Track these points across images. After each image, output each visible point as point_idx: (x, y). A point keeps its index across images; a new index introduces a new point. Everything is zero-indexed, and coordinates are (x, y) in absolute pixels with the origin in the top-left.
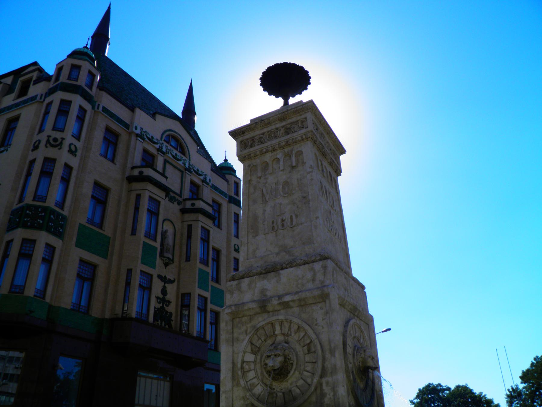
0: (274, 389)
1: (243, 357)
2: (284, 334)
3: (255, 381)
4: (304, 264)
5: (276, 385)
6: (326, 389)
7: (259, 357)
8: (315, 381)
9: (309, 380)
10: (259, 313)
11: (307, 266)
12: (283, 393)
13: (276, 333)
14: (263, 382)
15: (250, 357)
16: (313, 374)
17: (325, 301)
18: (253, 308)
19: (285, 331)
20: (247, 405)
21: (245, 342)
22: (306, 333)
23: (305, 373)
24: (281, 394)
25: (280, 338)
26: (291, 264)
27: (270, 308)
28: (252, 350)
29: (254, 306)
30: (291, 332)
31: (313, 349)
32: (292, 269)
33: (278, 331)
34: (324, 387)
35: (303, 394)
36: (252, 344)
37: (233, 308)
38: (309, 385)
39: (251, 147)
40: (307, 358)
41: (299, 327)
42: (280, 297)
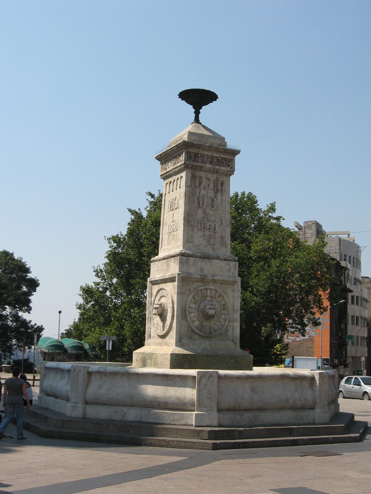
1: (190, 304)
3: (194, 318)
4: (225, 260)
6: (230, 329)
7: (197, 306)
8: (226, 324)
9: (223, 323)
14: (198, 320)
15: (193, 306)
16: (225, 320)
17: (234, 285)
19: (212, 295)
21: (191, 296)
22: (223, 299)
23: (221, 319)
24: (208, 328)
26: (218, 258)
28: (194, 301)
30: (216, 296)
34: (228, 327)
35: (219, 329)
36: (194, 298)
38: (223, 325)
39: (194, 161)
40: (222, 312)
41: (220, 295)
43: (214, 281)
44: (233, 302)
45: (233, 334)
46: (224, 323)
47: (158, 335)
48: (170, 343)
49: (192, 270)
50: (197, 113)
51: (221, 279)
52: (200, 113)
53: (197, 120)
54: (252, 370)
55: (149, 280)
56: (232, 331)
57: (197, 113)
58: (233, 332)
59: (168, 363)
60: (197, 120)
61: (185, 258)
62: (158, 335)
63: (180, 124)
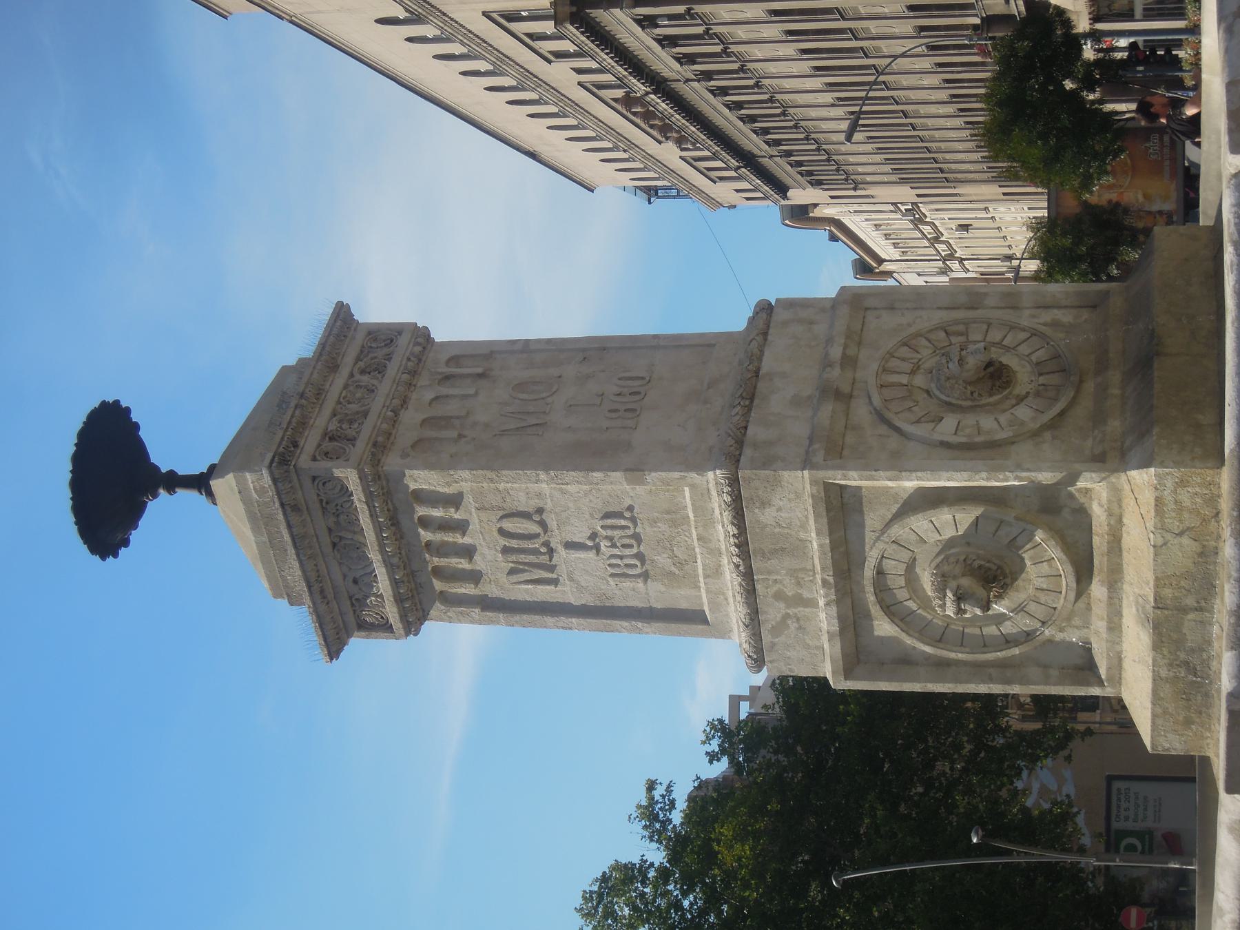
0: (1028, 393)
2: (913, 373)
5: (1019, 390)
6: (1047, 316)
10: (848, 408)
11: (771, 331)
12: (1041, 374)
13: (905, 381)
17: (867, 309)
18: (833, 411)
20: (1054, 438)
25: (919, 380)
27: (846, 388)
29: (831, 408)
31: (961, 328)
32: (767, 353)
33: (904, 379)
34: (1042, 321)
37: (816, 446)
38: (1032, 335)
41: (905, 344)
42: (827, 364)
43: (849, 362)
44: (939, 308)
45: (1066, 307)
46: (1024, 330)
47: (1076, 601)
48: (1110, 515)
49: (799, 429)
50: (173, 482)
51: (842, 341)
52: (172, 473)
53: (200, 483)
54: (1217, 229)
55: (839, 683)
56: (1056, 311)
57: (173, 482)
58: (1059, 307)
59: (1199, 475)
60: (200, 483)
61: (748, 452)
62: (1076, 601)
63: (206, 545)
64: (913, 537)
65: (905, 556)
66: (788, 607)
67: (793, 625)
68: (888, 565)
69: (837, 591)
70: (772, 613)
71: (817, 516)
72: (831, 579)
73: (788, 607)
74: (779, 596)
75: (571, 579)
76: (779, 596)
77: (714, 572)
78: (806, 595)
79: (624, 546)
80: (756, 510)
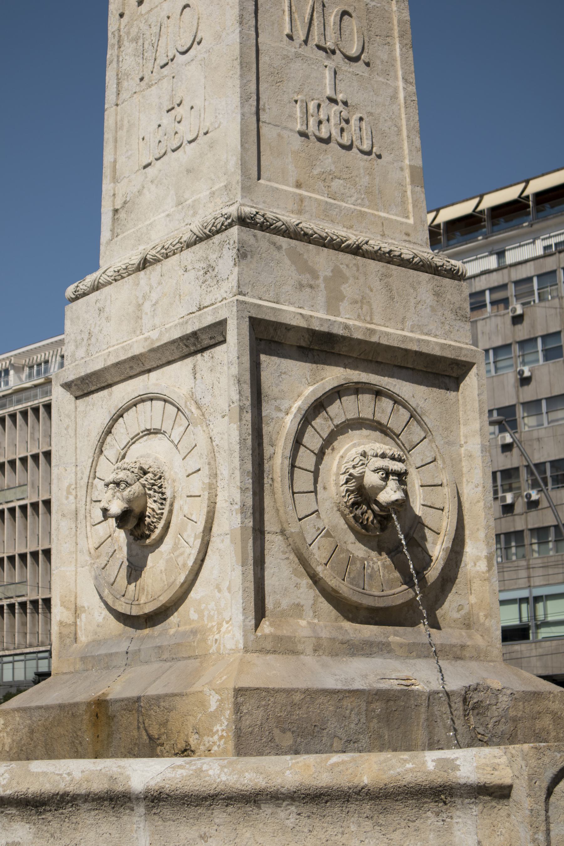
64: (416, 440)
65: (395, 424)
66: (326, 279)
67: (306, 278)
68: (386, 404)
69: (360, 342)
70: (323, 260)
71: (443, 346)
72: (374, 339)
73: (326, 279)
74: (338, 276)
75: (297, 56)
76: (338, 276)
77: (326, 212)
78: (344, 306)
79: (342, 130)
80: (430, 286)
